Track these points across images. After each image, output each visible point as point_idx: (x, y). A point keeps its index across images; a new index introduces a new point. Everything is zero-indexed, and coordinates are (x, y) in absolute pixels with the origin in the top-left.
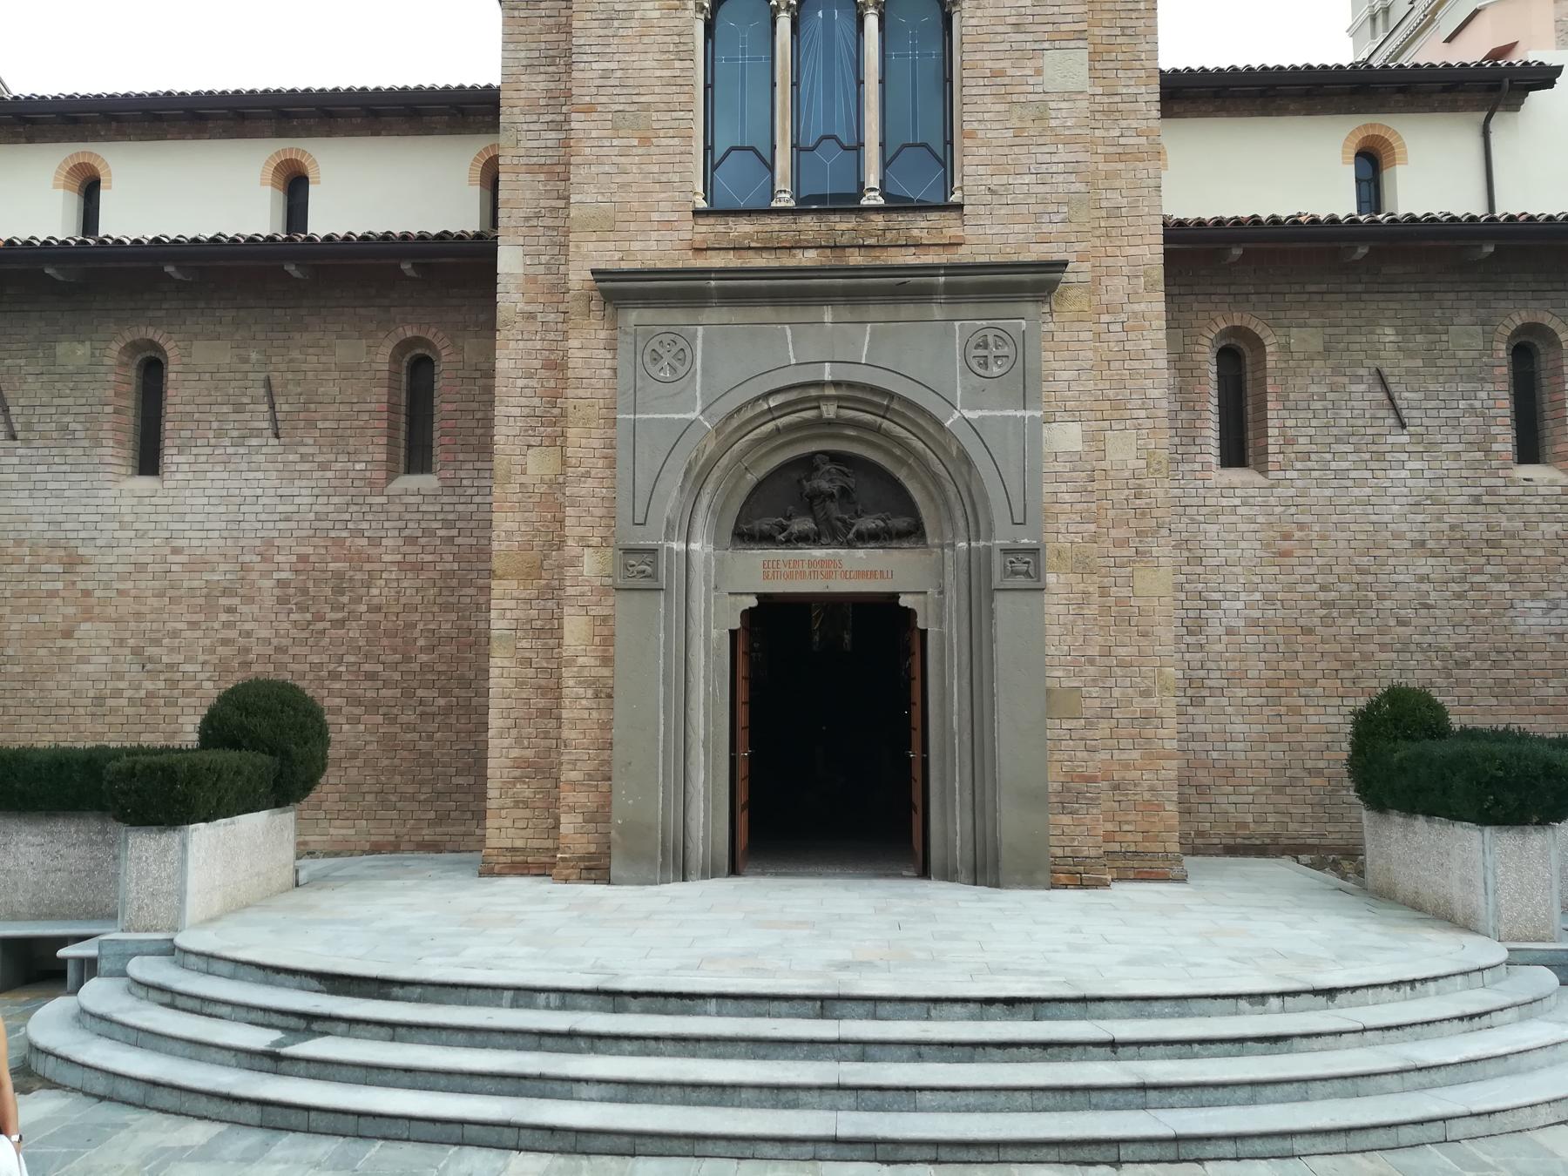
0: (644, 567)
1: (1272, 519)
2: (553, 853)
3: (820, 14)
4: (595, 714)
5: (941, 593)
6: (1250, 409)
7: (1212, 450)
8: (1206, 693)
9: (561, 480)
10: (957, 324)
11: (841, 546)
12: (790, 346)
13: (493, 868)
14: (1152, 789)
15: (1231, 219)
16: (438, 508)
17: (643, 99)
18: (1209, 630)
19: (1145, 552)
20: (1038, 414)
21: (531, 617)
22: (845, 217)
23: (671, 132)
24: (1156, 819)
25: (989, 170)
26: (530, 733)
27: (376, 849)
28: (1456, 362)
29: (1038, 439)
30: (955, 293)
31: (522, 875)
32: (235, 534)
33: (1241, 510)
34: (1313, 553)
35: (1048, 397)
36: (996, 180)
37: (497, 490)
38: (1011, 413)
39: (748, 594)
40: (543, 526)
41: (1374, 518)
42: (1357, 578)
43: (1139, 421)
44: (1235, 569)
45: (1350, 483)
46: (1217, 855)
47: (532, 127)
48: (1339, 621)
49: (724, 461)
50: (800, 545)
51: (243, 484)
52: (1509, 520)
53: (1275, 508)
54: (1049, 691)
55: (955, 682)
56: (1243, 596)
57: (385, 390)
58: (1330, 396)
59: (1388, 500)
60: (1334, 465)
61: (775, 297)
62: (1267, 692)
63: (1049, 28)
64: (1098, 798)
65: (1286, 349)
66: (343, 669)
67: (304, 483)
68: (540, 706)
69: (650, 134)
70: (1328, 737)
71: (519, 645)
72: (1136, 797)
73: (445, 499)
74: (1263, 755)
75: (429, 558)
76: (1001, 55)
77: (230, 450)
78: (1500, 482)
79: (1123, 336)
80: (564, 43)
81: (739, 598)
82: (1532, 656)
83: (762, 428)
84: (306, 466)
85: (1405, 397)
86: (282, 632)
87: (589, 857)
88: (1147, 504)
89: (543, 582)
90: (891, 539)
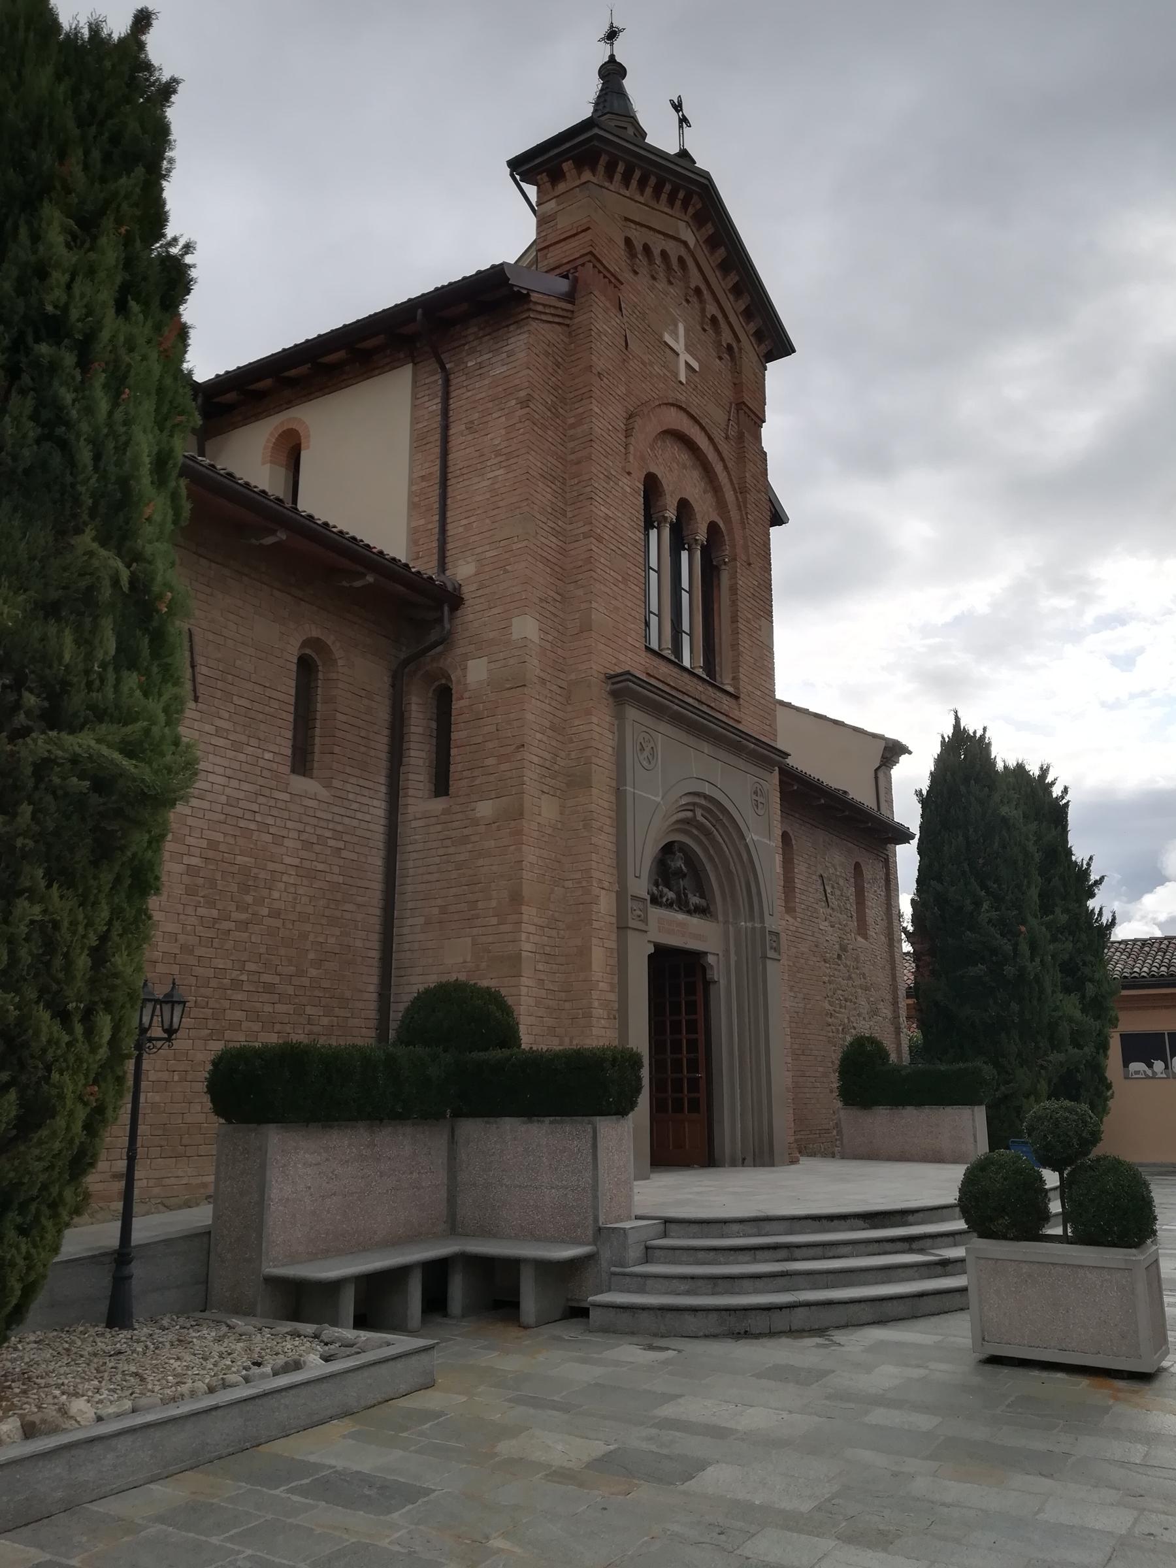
67: (218, 760)
73: (336, 809)
84: (221, 742)
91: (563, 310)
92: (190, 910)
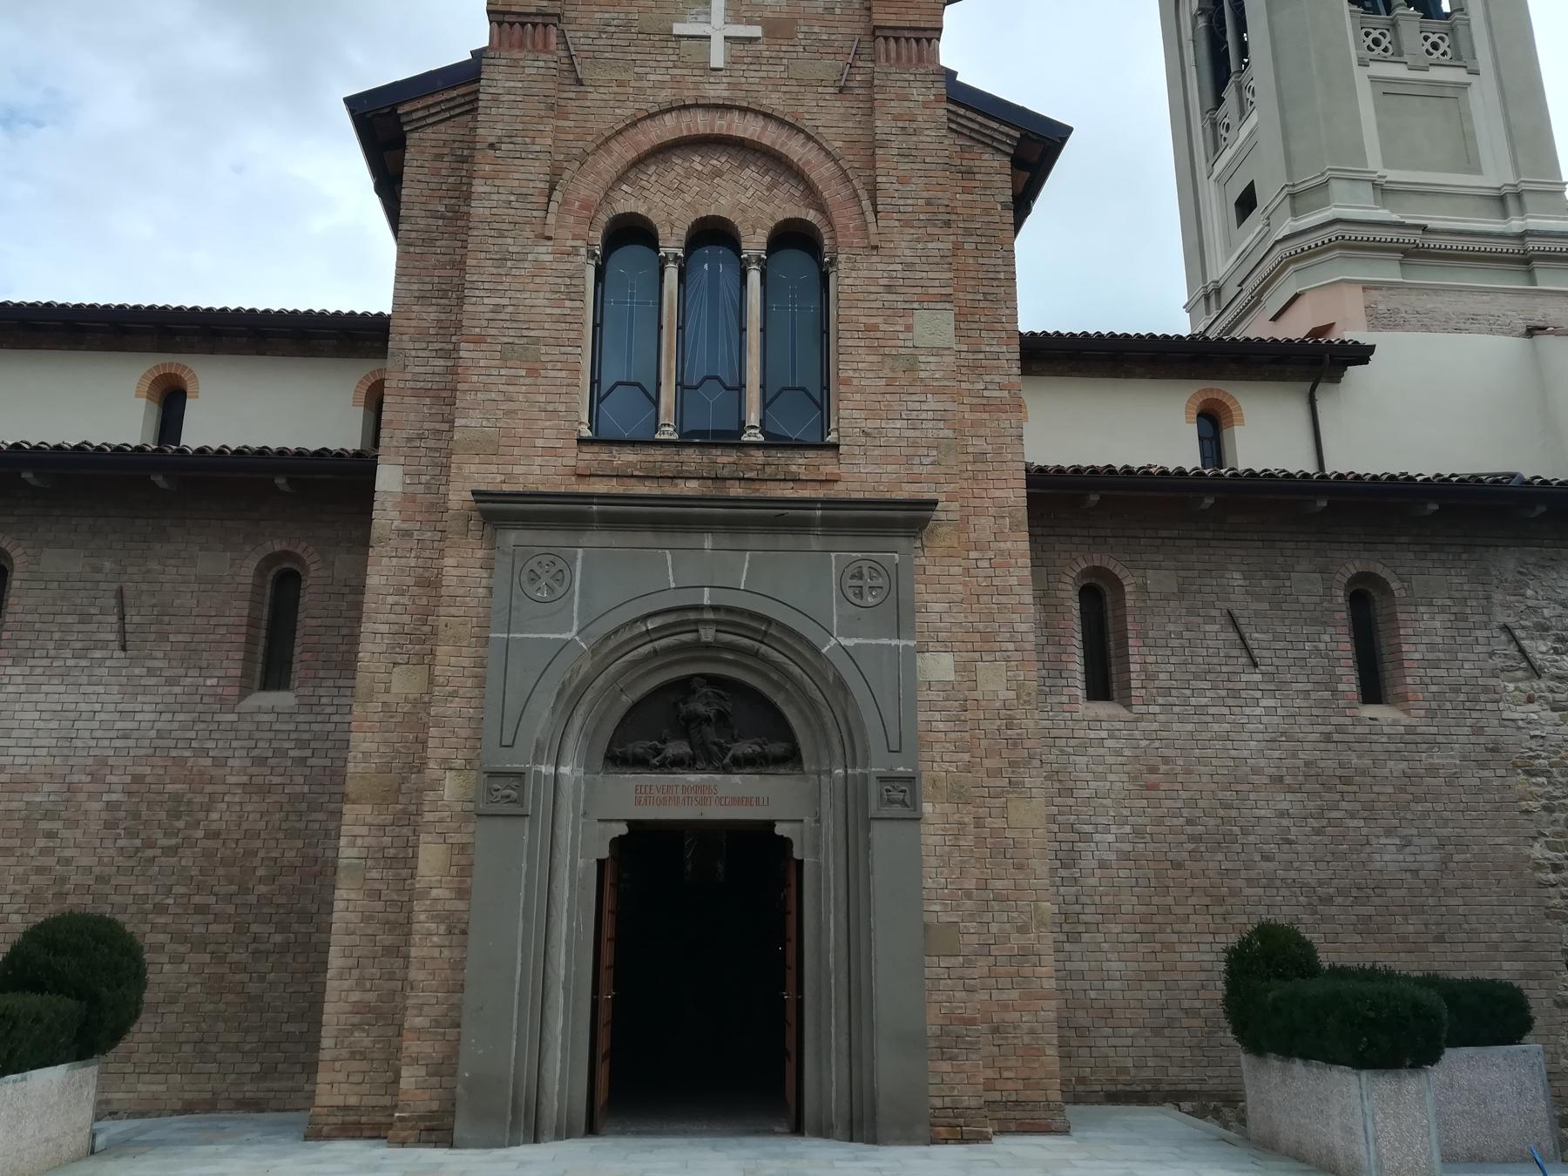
0: (508, 792)
1: (1138, 752)
2: (390, 1112)
3: (706, 266)
4: (446, 953)
5: (818, 821)
6: (1112, 644)
7: (1078, 683)
8: (1081, 928)
9: (426, 699)
10: (833, 555)
11: (717, 771)
12: (670, 570)
13: (321, 1131)
14: (1032, 1032)
15: (1088, 468)
16: (292, 727)
17: (532, 333)
18: (1083, 864)
19: (1017, 783)
20: (912, 643)
21: (384, 845)
22: (728, 451)
23: (559, 366)
24: (1036, 1065)
25: (863, 414)
26: (373, 974)
27: (188, 1108)
28: (1299, 607)
29: (912, 668)
30: (832, 526)
31: (353, 1138)
32: (66, 752)
33: (1108, 743)
34: (1179, 787)
35: (920, 627)
36: (870, 424)
37: (357, 709)
38: (885, 641)
39: (618, 820)
40: (404, 747)
41: (1233, 753)
42: (1221, 812)
43: (1009, 653)
44: (1104, 801)
45: (1209, 719)
46: (1099, 1103)
47: (420, 353)
48: (1207, 856)
49: (600, 682)
50: (674, 769)
51: (80, 698)
52: (1359, 757)
53: (1141, 742)
54: (926, 927)
55: (832, 916)
56: (1114, 829)
57: (246, 604)
58: (1186, 634)
59: (1246, 736)
60: (1193, 701)
61: (656, 524)
62: (1141, 928)
63: (919, 290)
64: (978, 1043)
65: (1143, 589)
66: (170, 901)
67: (148, 698)
68: (387, 943)
69: (537, 366)
70: (1203, 976)
71: (368, 876)
72: (1015, 1041)
73: (301, 718)
74: (1140, 995)
75: (276, 780)
76: (874, 312)
77: (70, 662)
78: (1348, 721)
79: (991, 572)
80: (457, 279)
81: (608, 825)
82: (1391, 892)
83: (639, 650)
84: (152, 681)
85: (1256, 637)
86: (106, 860)
87: (432, 1115)
88: (1018, 734)
89: (399, 807)
90: (768, 764)
91: (464, 95)
92: (108, 843)
